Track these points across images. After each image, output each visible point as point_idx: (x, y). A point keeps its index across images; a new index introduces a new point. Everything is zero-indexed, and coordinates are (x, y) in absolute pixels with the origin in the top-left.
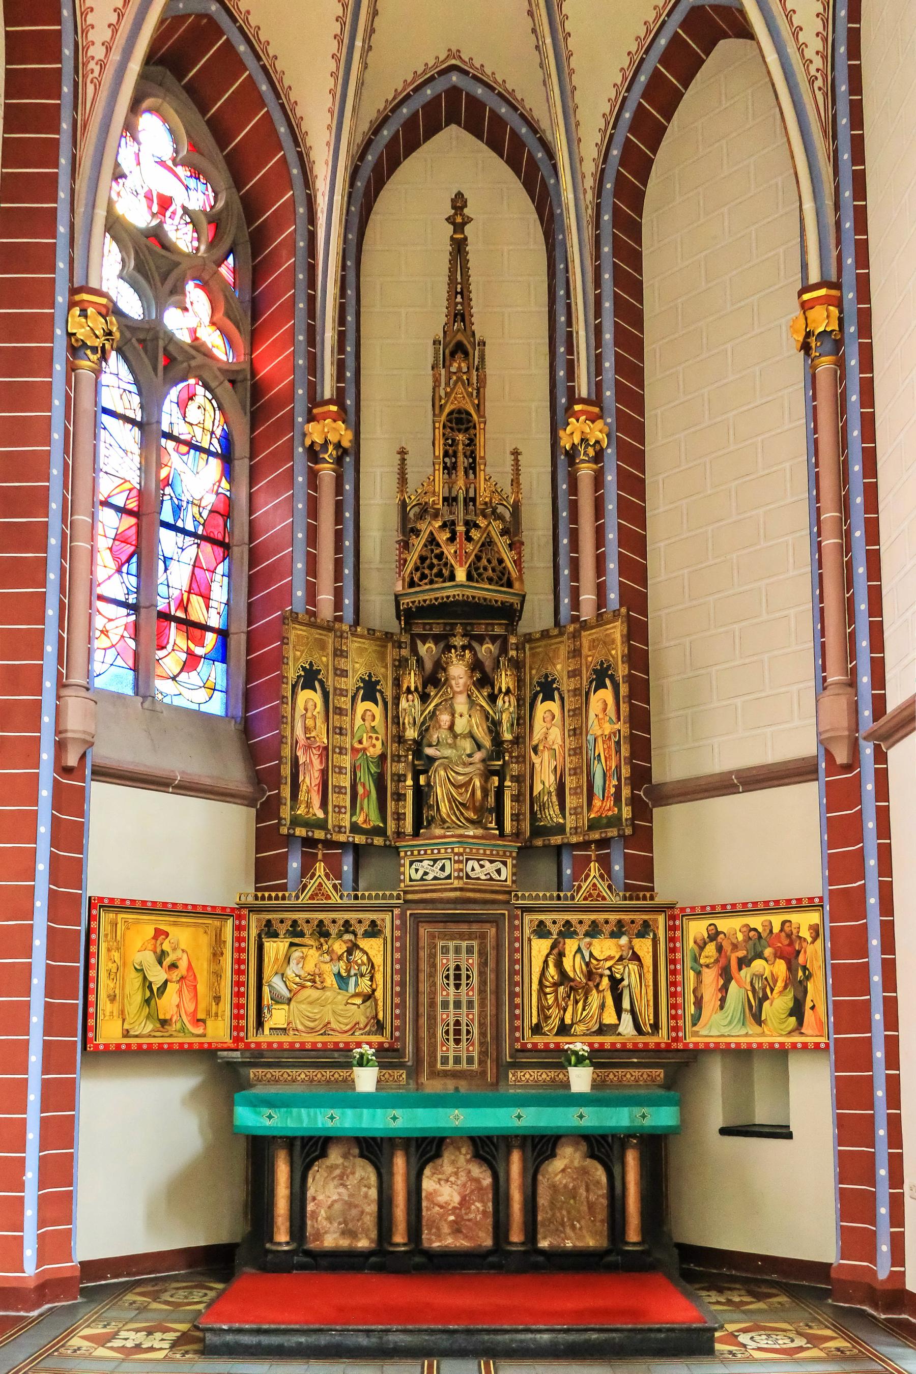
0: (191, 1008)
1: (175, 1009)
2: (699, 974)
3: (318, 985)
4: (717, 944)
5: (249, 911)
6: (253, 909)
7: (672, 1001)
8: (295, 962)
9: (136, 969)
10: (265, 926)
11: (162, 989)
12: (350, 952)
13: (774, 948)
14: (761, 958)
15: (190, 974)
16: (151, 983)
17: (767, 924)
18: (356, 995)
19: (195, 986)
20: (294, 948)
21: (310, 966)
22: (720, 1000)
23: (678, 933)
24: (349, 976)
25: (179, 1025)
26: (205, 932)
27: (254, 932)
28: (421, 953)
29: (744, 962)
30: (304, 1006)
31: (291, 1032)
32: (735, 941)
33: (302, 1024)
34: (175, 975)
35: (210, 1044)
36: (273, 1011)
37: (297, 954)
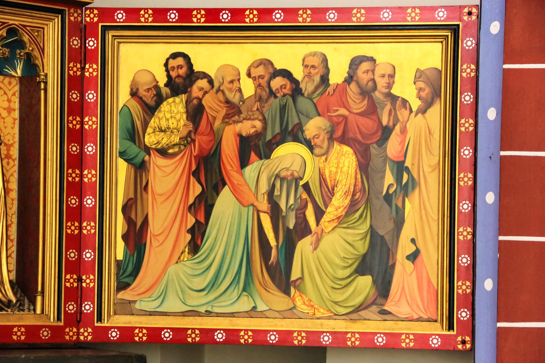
2: (140, 168)
4: (188, 102)
7: (71, 228)
13: (330, 119)
14: (296, 139)
17: (316, 61)
22: (191, 231)
23: (92, 70)
29: (254, 147)
32: (234, 98)
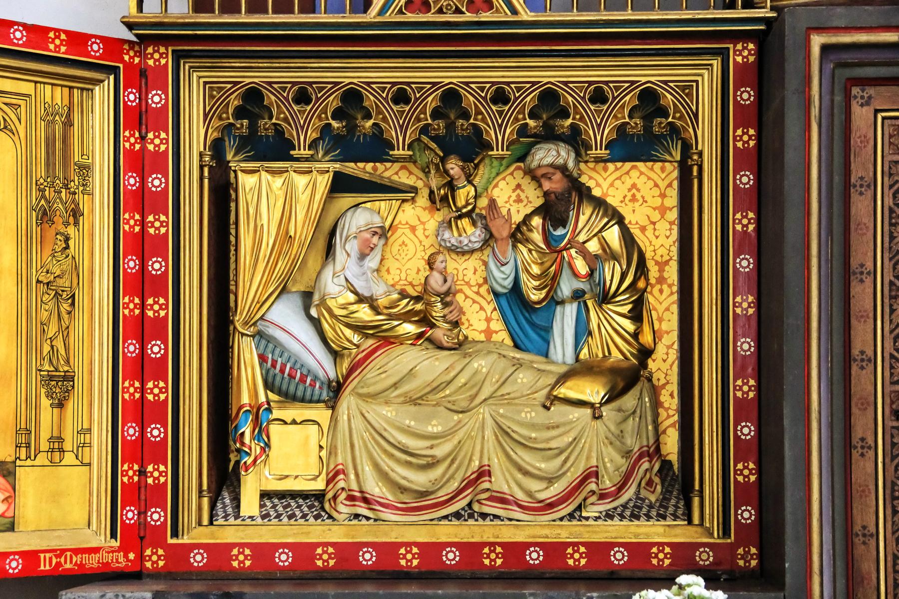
3: (440, 333)
5: (178, 56)
6: (190, 45)
8: (353, 247)
10: (240, 113)
12: (554, 212)
18: (582, 369)
20: (346, 200)
21: (407, 263)
24: (553, 301)
27: (197, 136)
28: (860, 206)
30: (388, 412)
31: (344, 509)
33: (384, 476)
35: (30, 557)
36: (274, 429)
37: (361, 217)
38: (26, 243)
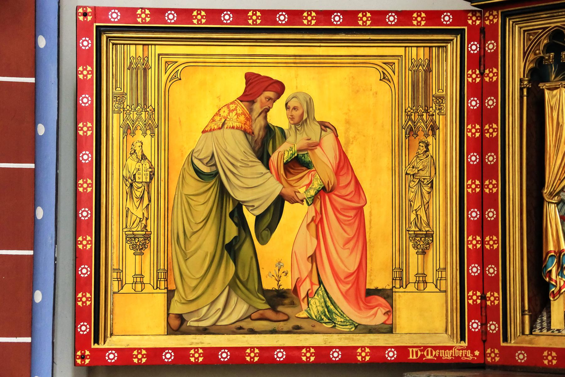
0: (348, 262)
1: (306, 267)
5: (505, 16)
9: (198, 172)
11: (268, 219)
15: (344, 180)
16: (239, 206)
19: (360, 211)
25: (316, 306)
26: (384, 78)
27: (517, 67)
34: (305, 185)
35: (403, 350)
38: (397, 151)
